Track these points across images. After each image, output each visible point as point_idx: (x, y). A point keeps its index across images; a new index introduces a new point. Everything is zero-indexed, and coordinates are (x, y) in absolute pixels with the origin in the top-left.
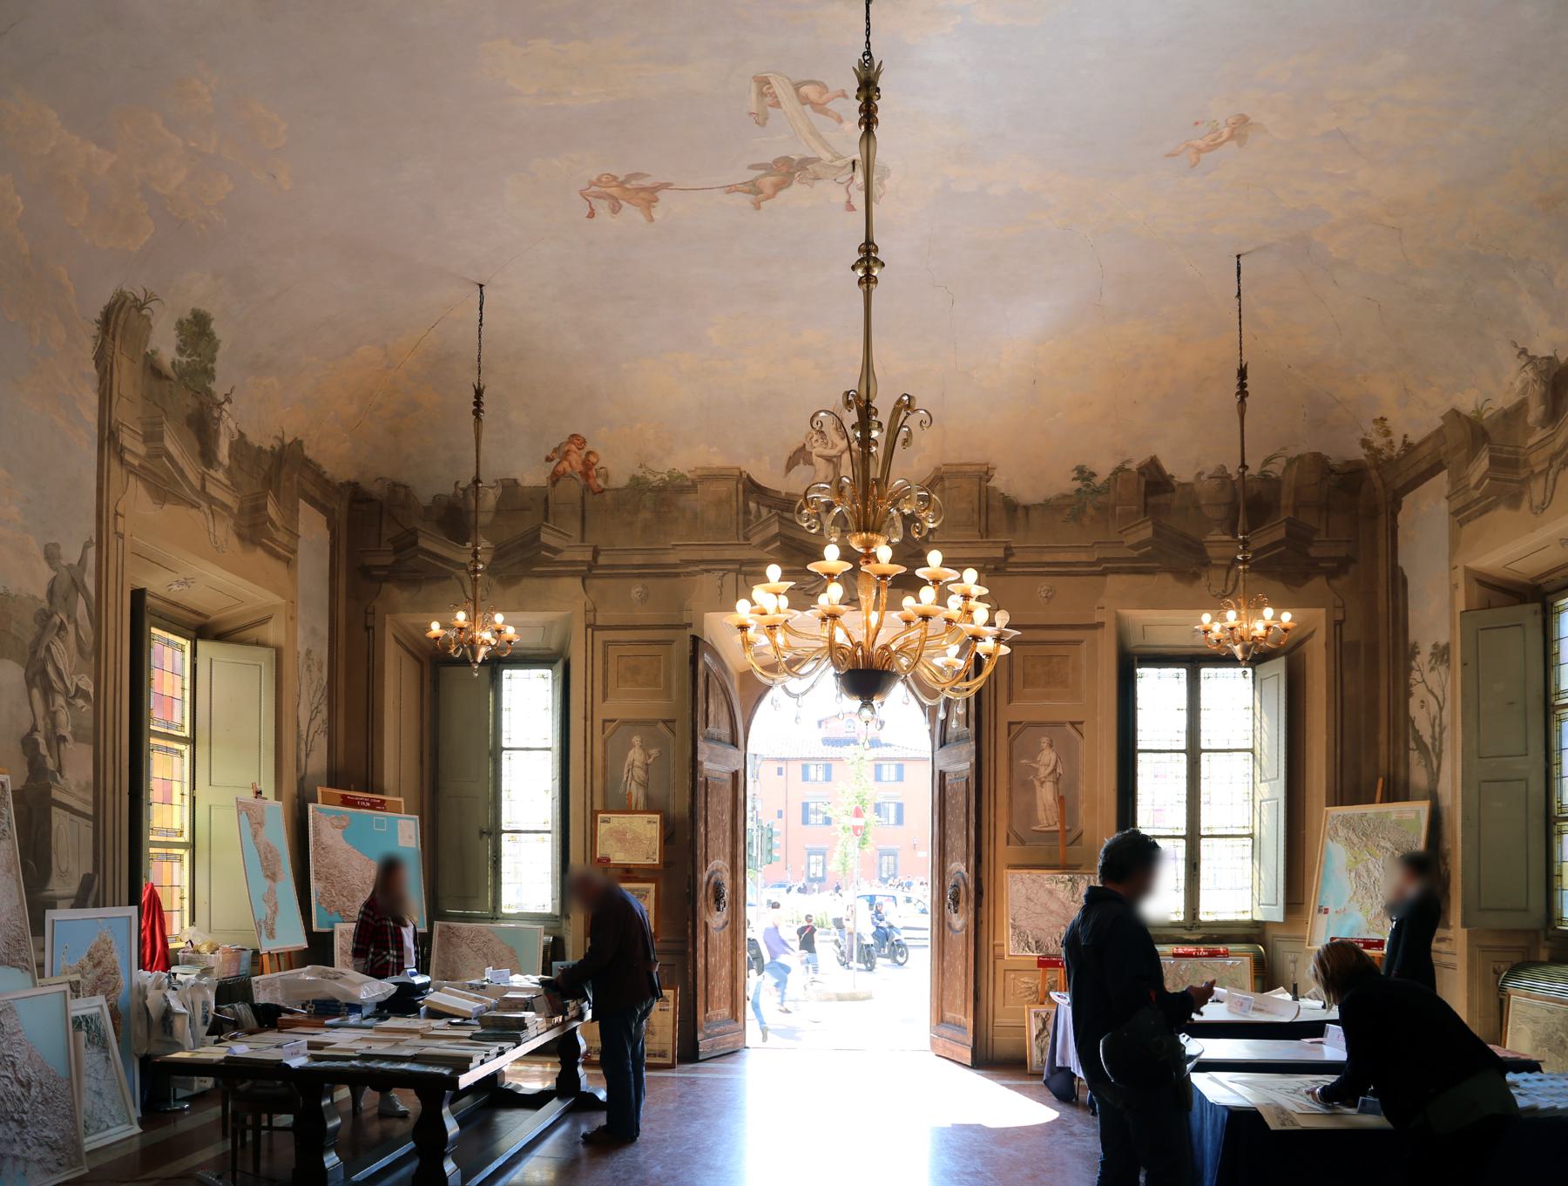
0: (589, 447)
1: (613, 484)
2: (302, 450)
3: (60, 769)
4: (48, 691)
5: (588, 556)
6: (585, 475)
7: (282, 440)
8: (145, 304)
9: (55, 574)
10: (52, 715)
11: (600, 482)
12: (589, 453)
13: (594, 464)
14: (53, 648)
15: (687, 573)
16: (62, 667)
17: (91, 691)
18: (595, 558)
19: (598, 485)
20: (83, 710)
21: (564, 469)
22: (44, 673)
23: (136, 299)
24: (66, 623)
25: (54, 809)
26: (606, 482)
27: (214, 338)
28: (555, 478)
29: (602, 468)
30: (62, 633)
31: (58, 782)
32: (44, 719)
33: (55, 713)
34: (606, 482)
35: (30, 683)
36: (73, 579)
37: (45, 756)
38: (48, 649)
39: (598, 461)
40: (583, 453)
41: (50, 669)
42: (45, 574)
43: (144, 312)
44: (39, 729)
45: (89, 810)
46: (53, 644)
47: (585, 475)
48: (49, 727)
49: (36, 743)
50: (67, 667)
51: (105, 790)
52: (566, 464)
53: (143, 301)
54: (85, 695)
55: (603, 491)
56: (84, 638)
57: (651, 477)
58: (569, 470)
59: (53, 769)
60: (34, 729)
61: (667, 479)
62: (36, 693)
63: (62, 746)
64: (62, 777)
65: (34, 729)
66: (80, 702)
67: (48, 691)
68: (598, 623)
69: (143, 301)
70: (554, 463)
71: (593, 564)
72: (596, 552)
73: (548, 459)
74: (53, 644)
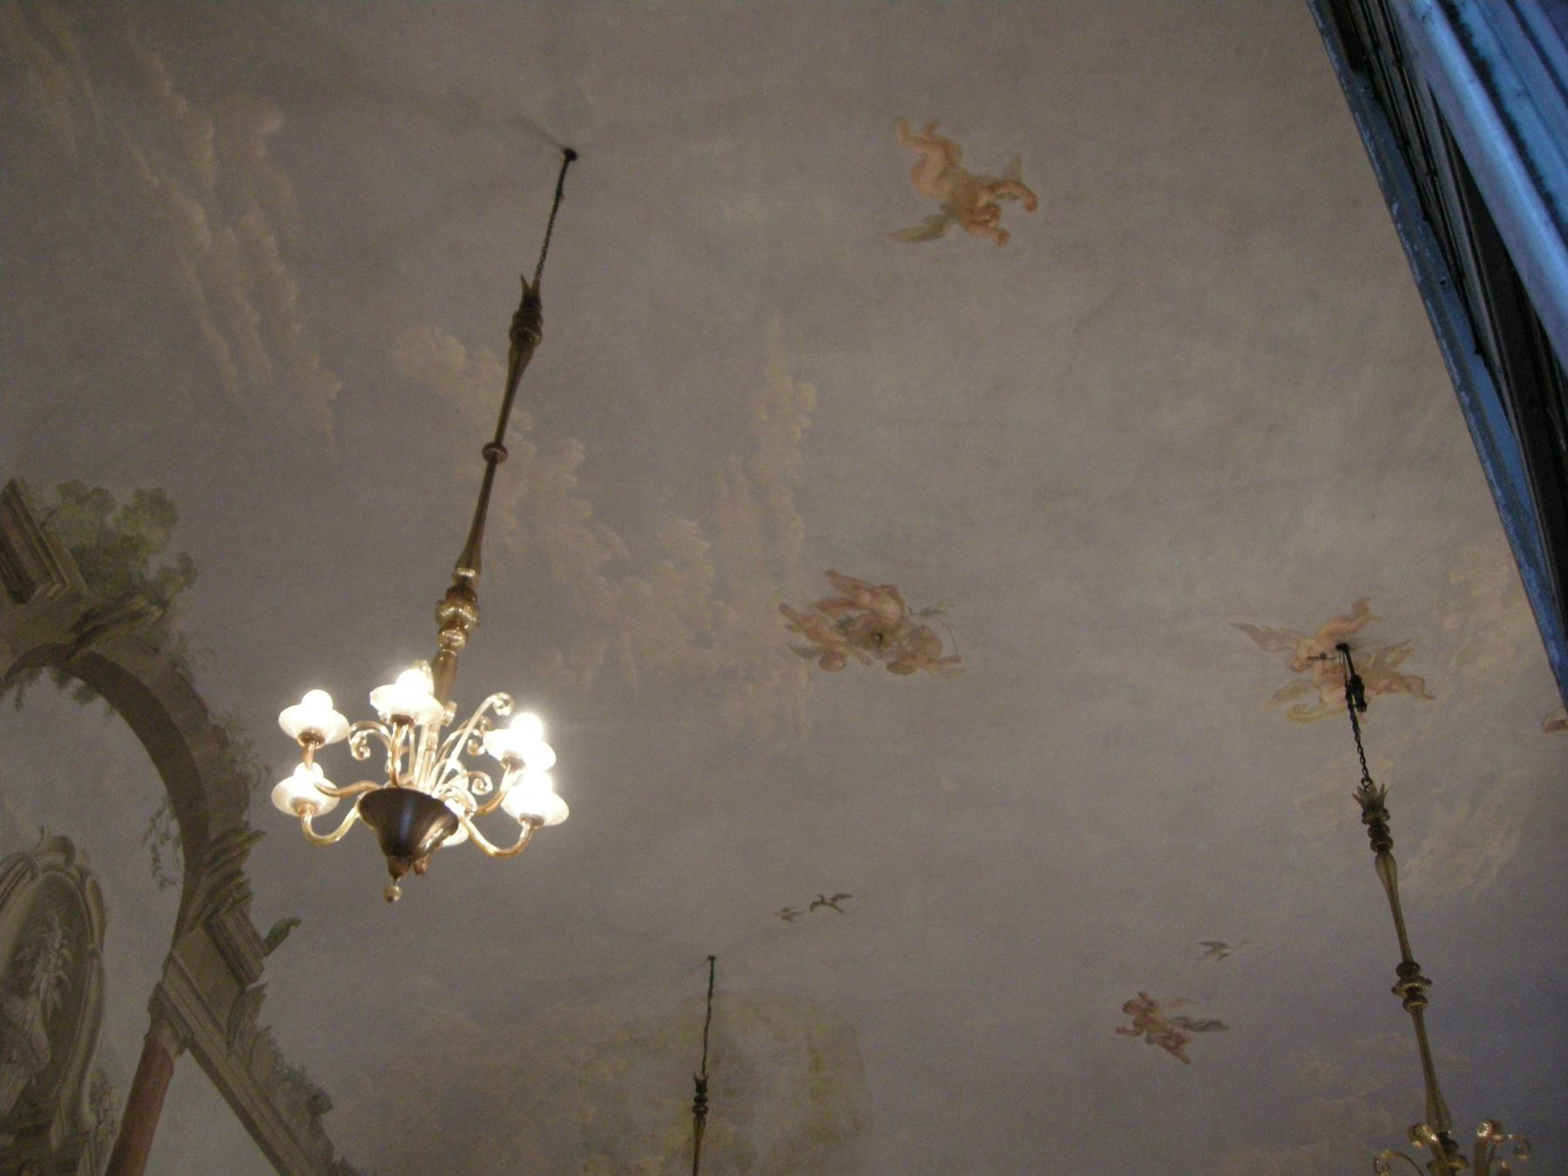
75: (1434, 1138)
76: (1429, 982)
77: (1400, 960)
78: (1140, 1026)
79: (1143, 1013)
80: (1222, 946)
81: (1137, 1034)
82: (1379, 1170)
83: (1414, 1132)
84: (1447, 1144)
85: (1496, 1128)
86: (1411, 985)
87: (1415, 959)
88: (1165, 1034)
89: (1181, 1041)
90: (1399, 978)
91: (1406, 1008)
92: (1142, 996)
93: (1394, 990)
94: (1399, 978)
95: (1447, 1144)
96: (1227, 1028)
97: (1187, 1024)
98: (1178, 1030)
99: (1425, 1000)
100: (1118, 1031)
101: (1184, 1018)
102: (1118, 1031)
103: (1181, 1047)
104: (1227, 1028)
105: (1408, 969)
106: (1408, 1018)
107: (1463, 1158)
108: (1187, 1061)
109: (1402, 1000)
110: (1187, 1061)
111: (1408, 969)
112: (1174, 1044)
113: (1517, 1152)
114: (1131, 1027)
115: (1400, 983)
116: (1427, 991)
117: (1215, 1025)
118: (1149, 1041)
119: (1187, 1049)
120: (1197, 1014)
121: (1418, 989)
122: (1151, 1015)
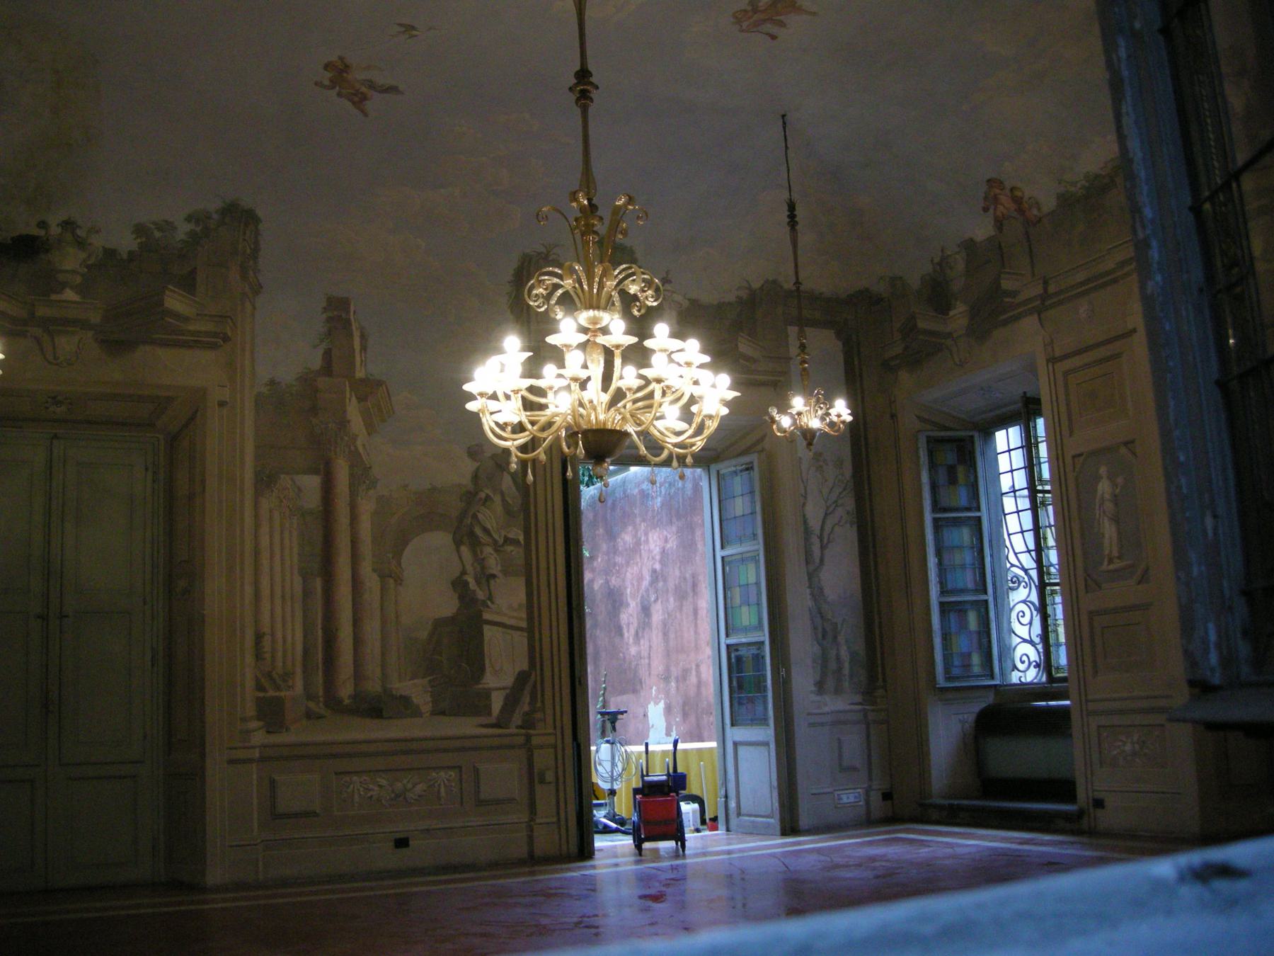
0: (1008, 185)
1: (1045, 209)
2: (781, 287)
3: (490, 598)
4: (475, 543)
5: (1039, 290)
6: (1021, 211)
7: (750, 288)
8: (549, 252)
9: (476, 465)
10: (480, 561)
11: (1035, 212)
12: (1012, 190)
13: (1022, 198)
14: (480, 516)
15: (1125, 274)
16: (489, 527)
17: (521, 538)
18: (1045, 290)
19: (1036, 216)
20: (513, 553)
21: (1002, 213)
22: (472, 534)
23: (539, 254)
24: (492, 496)
25: (486, 628)
26: (1039, 209)
27: (626, 247)
28: (999, 223)
29: (1030, 198)
30: (488, 503)
31: (488, 607)
32: (472, 565)
33: (483, 559)
34: (1039, 209)
35: (458, 543)
36: (497, 464)
37: (474, 591)
38: (475, 517)
39: (1023, 193)
40: (1008, 192)
41: (478, 531)
42: (468, 466)
43: (550, 258)
44: (468, 572)
45: (524, 624)
46: (479, 512)
47: (1021, 211)
48: (478, 569)
49: (466, 583)
50: (495, 525)
51: (540, 609)
52: (1001, 208)
53: (545, 251)
54: (515, 542)
55: (1040, 220)
56: (511, 502)
57: (1073, 189)
58: (1005, 211)
59: (483, 598)
60: (464, 573)
61: (1087, 184)
62: (465, 550)
63: (492, 582)
64: (493, 603)
65: (464, 573)
66: (509, 548)
67: (475, 543)
68: (1057, 354)
69: (545, 251)
70: (991, 211)
71: (1045, 296)
72: (1046, 283)
73: (986, 210)
74: (479, 512)
75: (586, 202)
76: (597, 88)
77: (578, 68)
78: (334, 83)
79: (339, 72)
80: (413, 28)
81: (333, 88)
82: (540, 219)
83: (573, 196)
84: (593, 207)
85: (631, 200)
86: (582, 87)
87: (590, 69)
88: (353, 92)
89: (364, 98)
90: (576, 81)
91: (577, 104)
92: (341, 58)
93: (570, 89)
94: (576, 81)
95: (593, 207)
96: (402, 93)
97: (372, 85)
98: (364, 89)
99: (591, 100)
100: (316, 84)
101: (370, 81)
102: (316, 84)
103: (364, 103)
104: (402, 93)
105: (583, 75)
106: (578, 111)
107: (601, 218)
108: (366, 115)
109: (576, 98)
110: (366, 115)
111: (583, 75)
112: (359, 100)
113: (638, 218)
114: (327, 82)
115: (576, 85)
116: (595, 94)
117: (392, 89)
118: (339, 95)
119: (369, 105)
120: (381, 80)
121: (589, 92)
122: (345, 75)
